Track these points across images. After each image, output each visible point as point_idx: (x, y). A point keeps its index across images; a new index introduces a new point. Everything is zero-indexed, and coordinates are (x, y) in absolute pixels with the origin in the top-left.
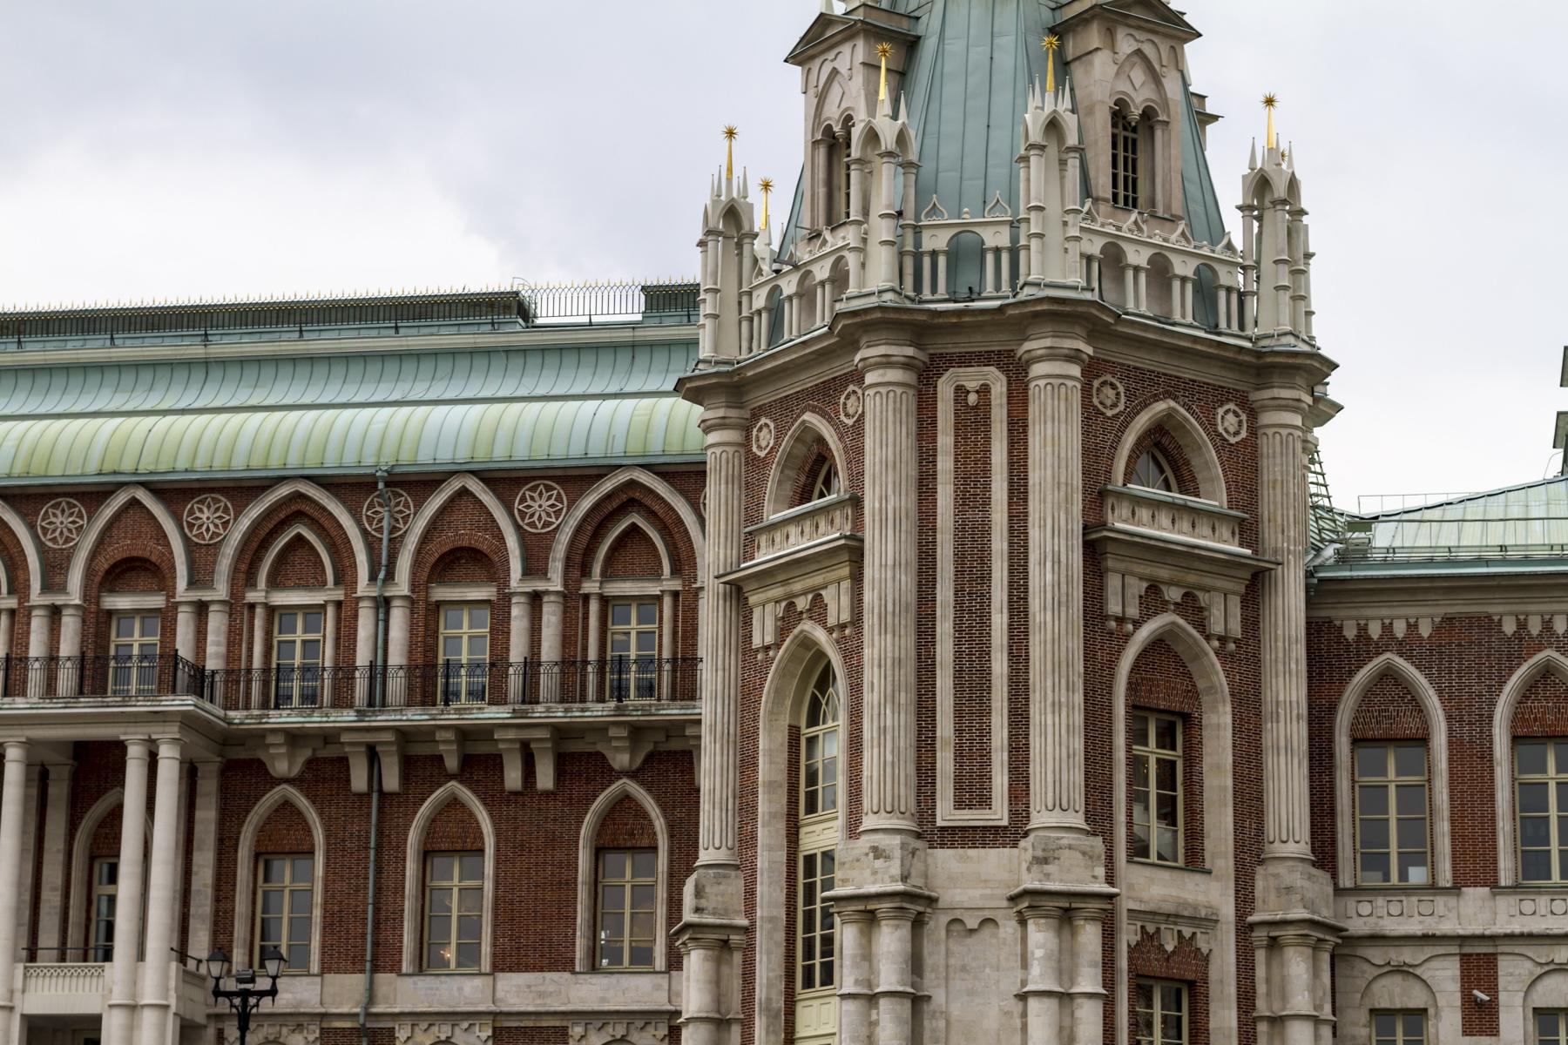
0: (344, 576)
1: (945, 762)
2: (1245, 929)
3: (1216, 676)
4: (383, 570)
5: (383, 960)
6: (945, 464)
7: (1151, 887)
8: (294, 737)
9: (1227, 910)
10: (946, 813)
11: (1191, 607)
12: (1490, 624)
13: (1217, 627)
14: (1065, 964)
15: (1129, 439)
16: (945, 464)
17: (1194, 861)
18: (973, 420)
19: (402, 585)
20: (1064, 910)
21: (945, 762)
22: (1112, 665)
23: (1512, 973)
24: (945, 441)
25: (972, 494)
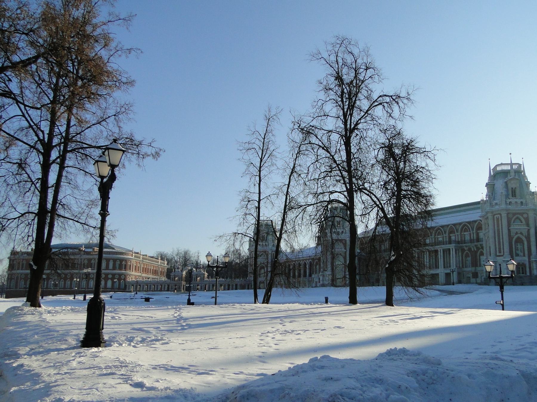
0: (470, 231)
1: (497, 249)
2: (529, 262)
3: (524, 239)
4: (473, 230)
5: (476, 266)
6: (496, 224)
8: (466, 246)
9: (527, 260)
10: (498, 254)
11: (521, 233)
15: (513, 219)
16: (496, 224)
17: (524, 256)
18: (498, 219)
19: (474, 231)
21: (497, 249)
22: (512, 240)
25: (498, 226)
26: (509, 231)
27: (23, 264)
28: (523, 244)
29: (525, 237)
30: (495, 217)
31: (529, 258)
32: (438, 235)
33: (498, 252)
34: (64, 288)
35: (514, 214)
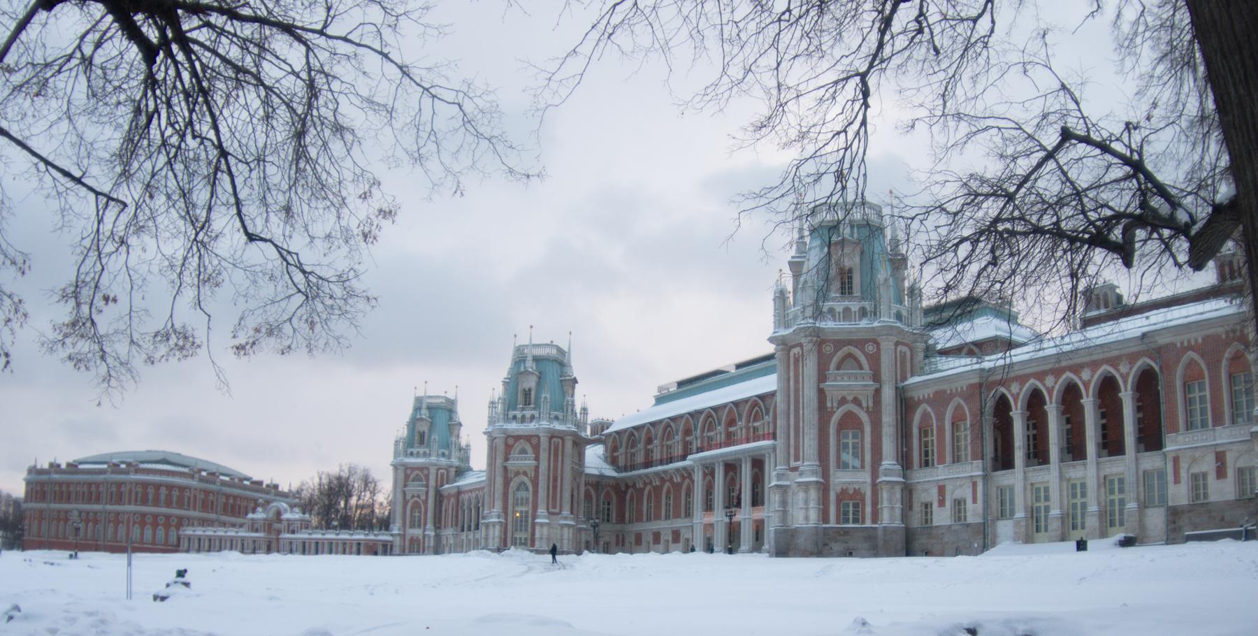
2: (874, 485)
3: (864, 417)
6: (792, 374)
7: (840, 479)
11: (856, 401)
12: (944, 392)
13: (864, 405)
14: (806, 502)
15: (835, 360)
16: (792, 374)
20: (805, 486)
23: (949, 488)
24: (792, 368)
25: (797, 382)
26: (821, 393)
27: (137, 494)
28: (863, 432)
29: (867, 411)
30: (792, 354)
31: (875, 474)
32: (755, 420)
33: (792, 458)
34: (142, 542)
35: (839, 344)
